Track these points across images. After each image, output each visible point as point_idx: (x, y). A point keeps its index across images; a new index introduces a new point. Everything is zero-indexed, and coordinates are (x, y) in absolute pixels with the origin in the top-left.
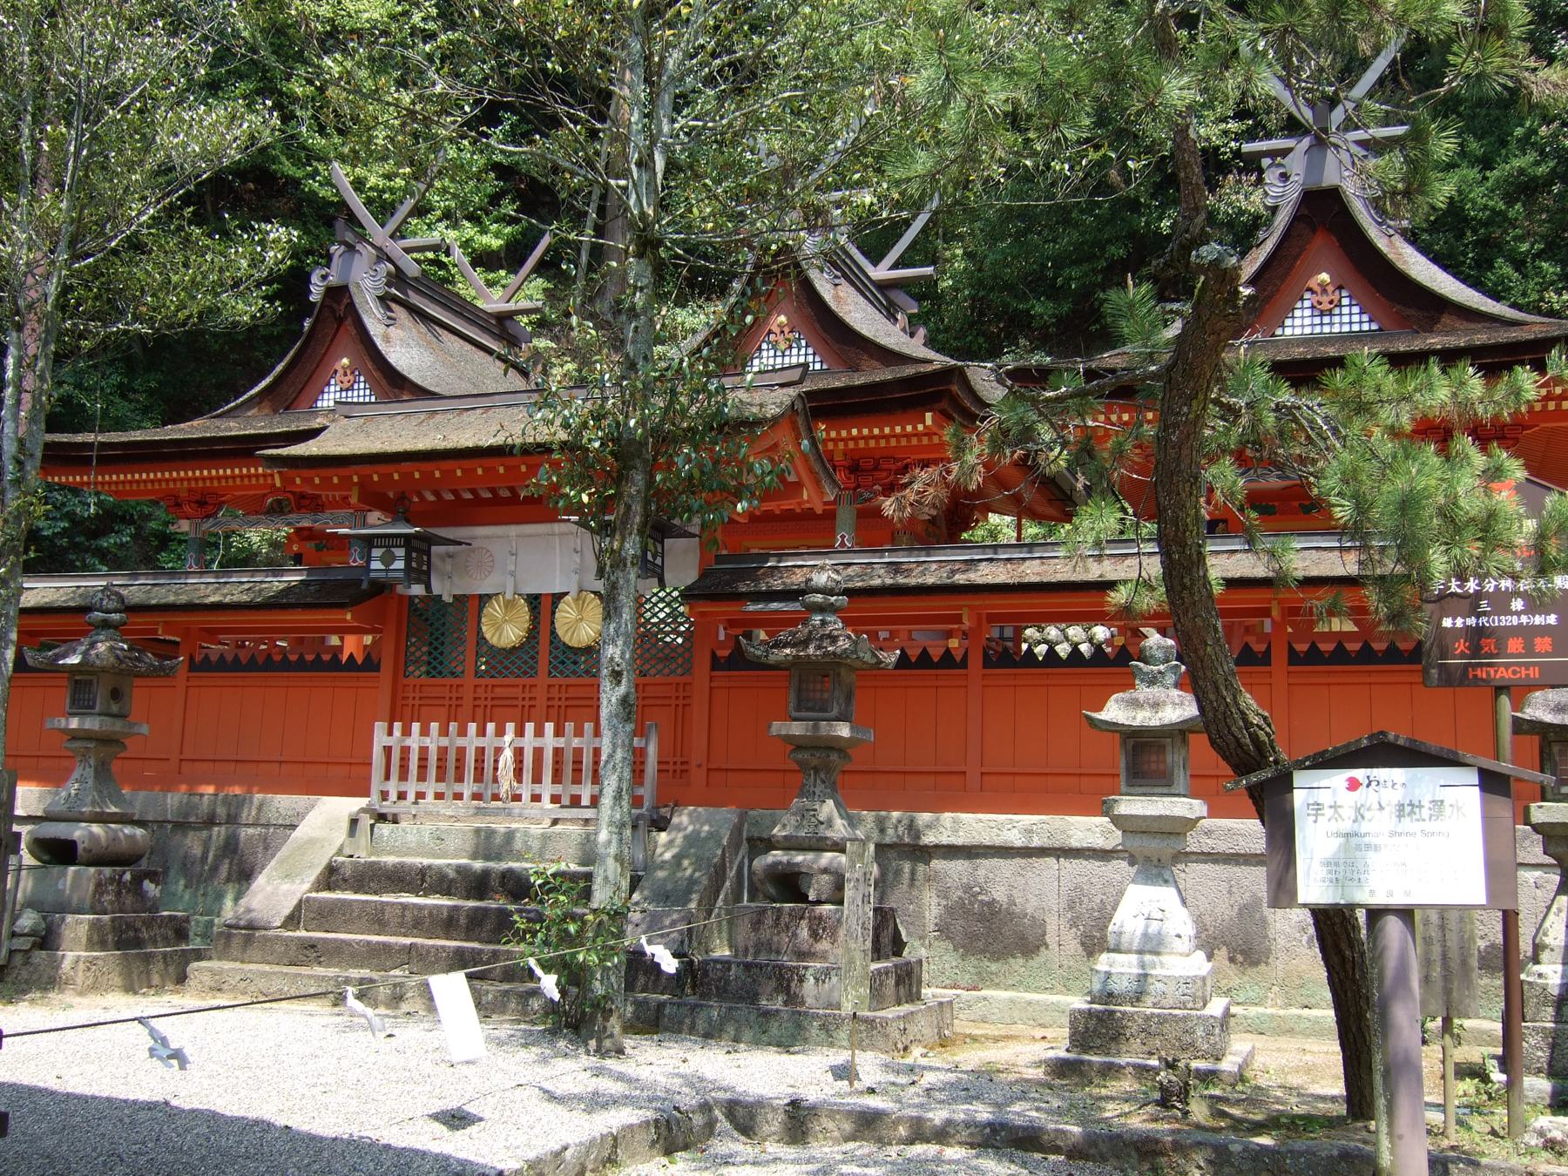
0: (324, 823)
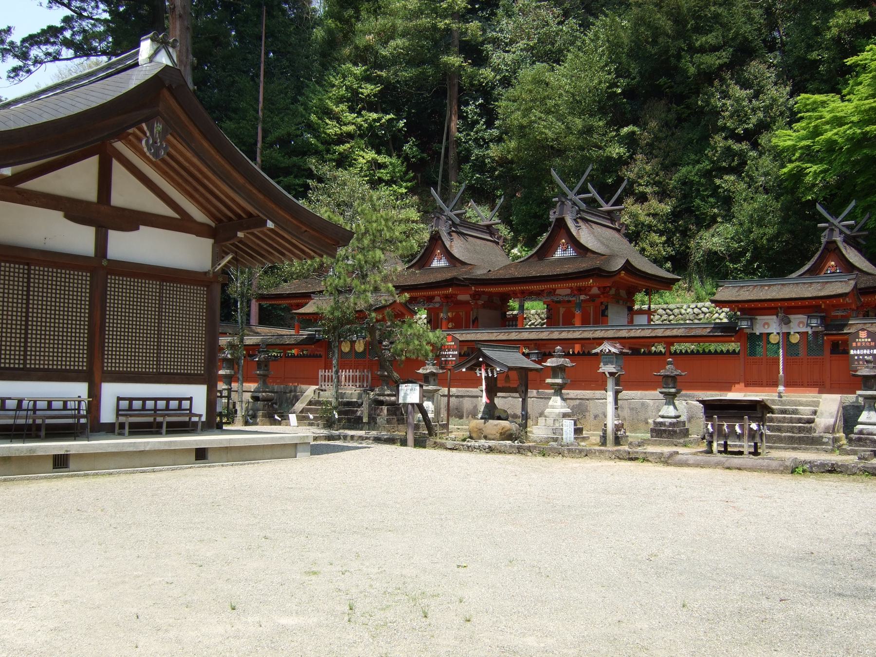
0: (309, 391)
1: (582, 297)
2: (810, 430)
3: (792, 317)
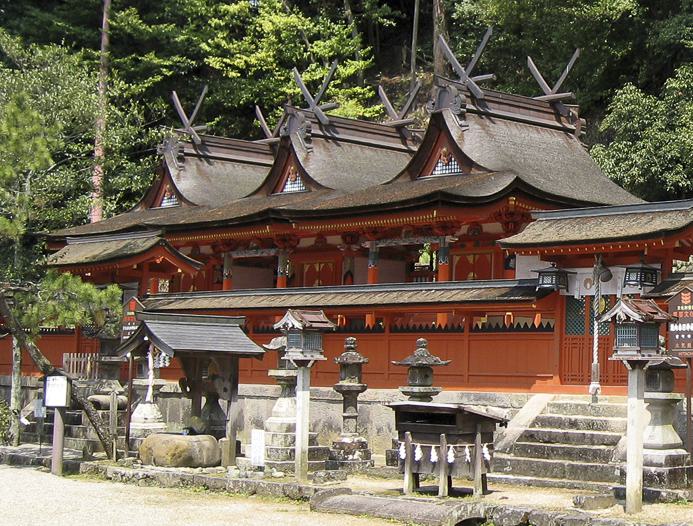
1: (449, 239)
2: (606, 457)
3: (612, 269)
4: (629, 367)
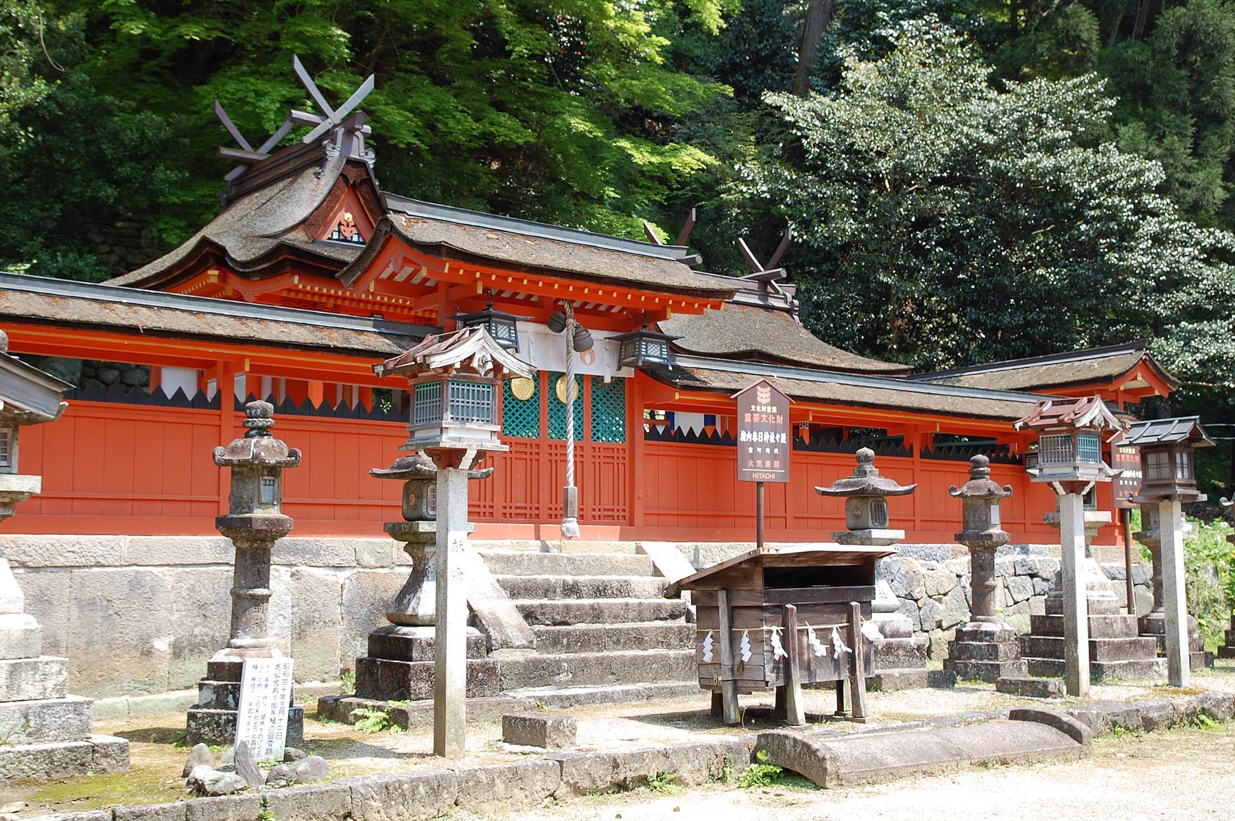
4: (1061, 490)
